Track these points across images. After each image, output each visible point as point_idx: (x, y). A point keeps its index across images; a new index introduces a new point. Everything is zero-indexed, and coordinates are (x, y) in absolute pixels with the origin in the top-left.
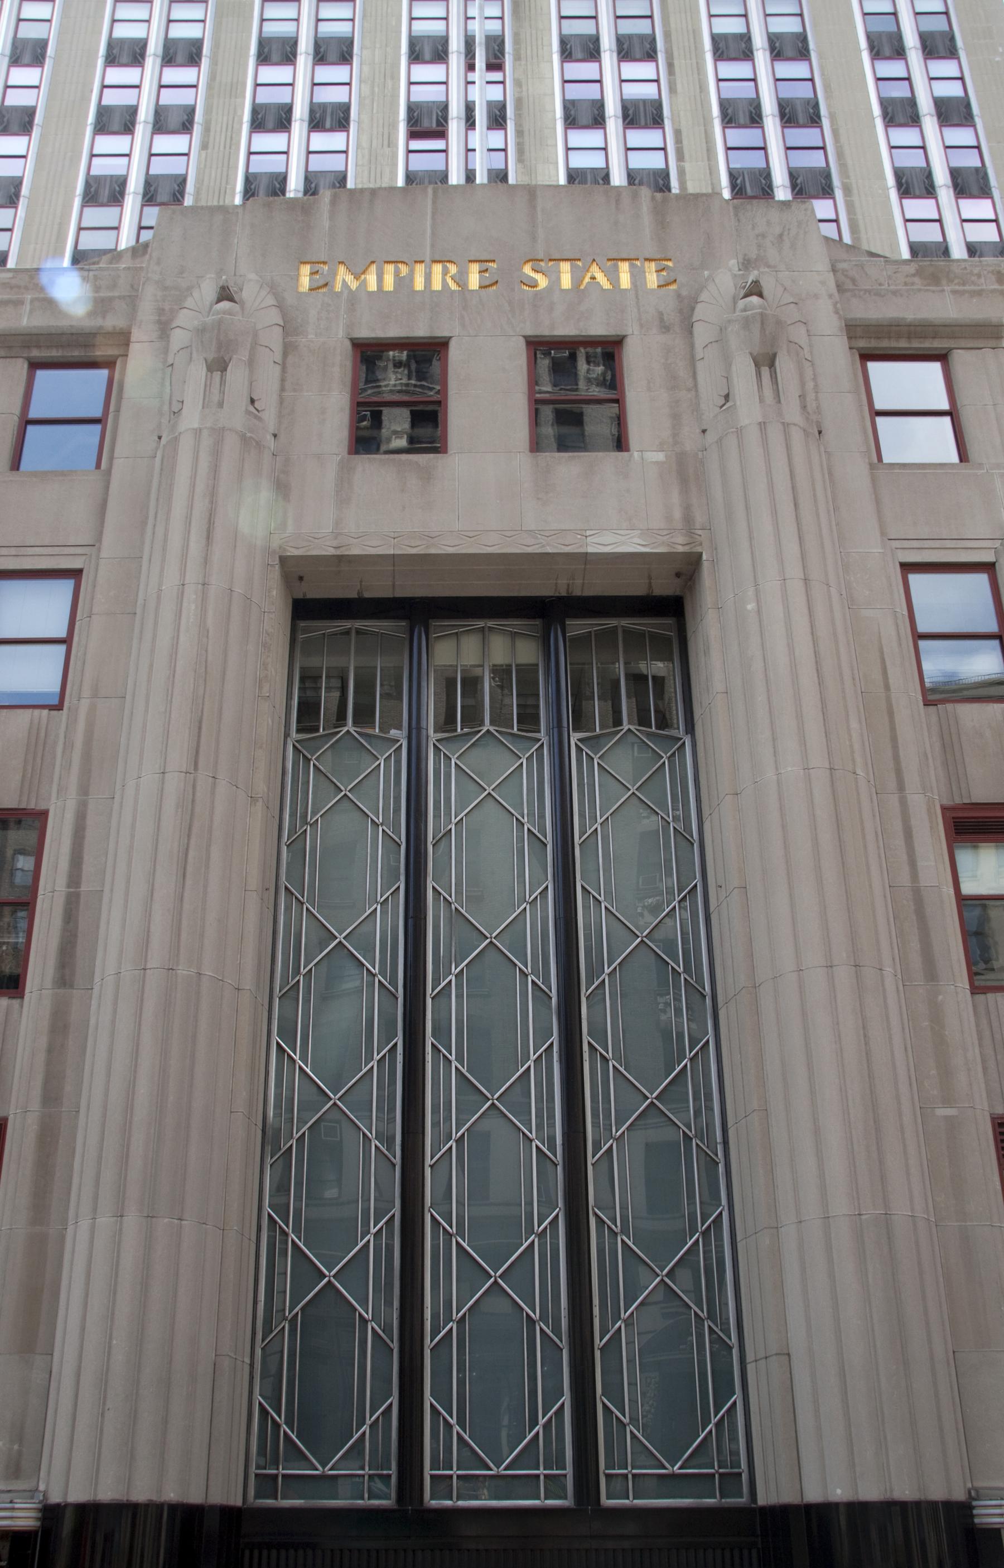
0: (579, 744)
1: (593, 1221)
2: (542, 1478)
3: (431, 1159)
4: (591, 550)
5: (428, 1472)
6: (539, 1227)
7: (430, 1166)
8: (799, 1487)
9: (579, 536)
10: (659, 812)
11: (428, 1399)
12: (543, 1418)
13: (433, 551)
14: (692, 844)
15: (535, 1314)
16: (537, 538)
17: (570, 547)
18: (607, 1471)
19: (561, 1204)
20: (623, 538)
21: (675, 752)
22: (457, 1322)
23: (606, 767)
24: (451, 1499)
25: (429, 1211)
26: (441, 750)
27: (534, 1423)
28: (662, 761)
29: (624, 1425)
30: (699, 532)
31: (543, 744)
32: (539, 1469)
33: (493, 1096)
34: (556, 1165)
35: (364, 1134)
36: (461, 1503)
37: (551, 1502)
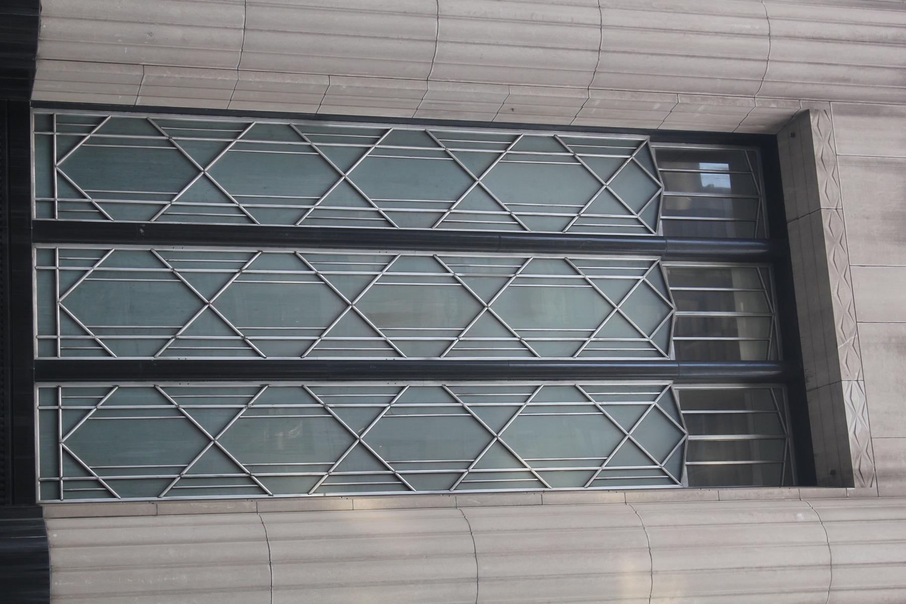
0: (667, 388)
1: (257, 384)
2: (55, 337)
3: (300, 254)
4: (845, 385)
5: (58, 247)
6: (250, 340)
7: (295, 252)
8: (55, 517)
9: (857, 374)
10: (611, 458)
11: (113, 248)
12: (100, 339)
13: (827, 243)
14: (583, 486)
15: (180, 335)
16: (850, 335)
17: (845, 365)
18: (60, 388)
19: (268, 358)
20: (860, 414)
21: (667, 475)
22: (172, 272)
23: (648, 412)
24: (37, 265)
25: (259, 251)
26: (650, 267)
27: (98, 331)
28: (658, 463)
29: (96, 405)
30: (874, 484)
31: (664, 356)
32: (61, 335)
33: (355, 305)
34: (301, 356)
35: (318, 200)
36: (35, 272)
37: (36, 343)
